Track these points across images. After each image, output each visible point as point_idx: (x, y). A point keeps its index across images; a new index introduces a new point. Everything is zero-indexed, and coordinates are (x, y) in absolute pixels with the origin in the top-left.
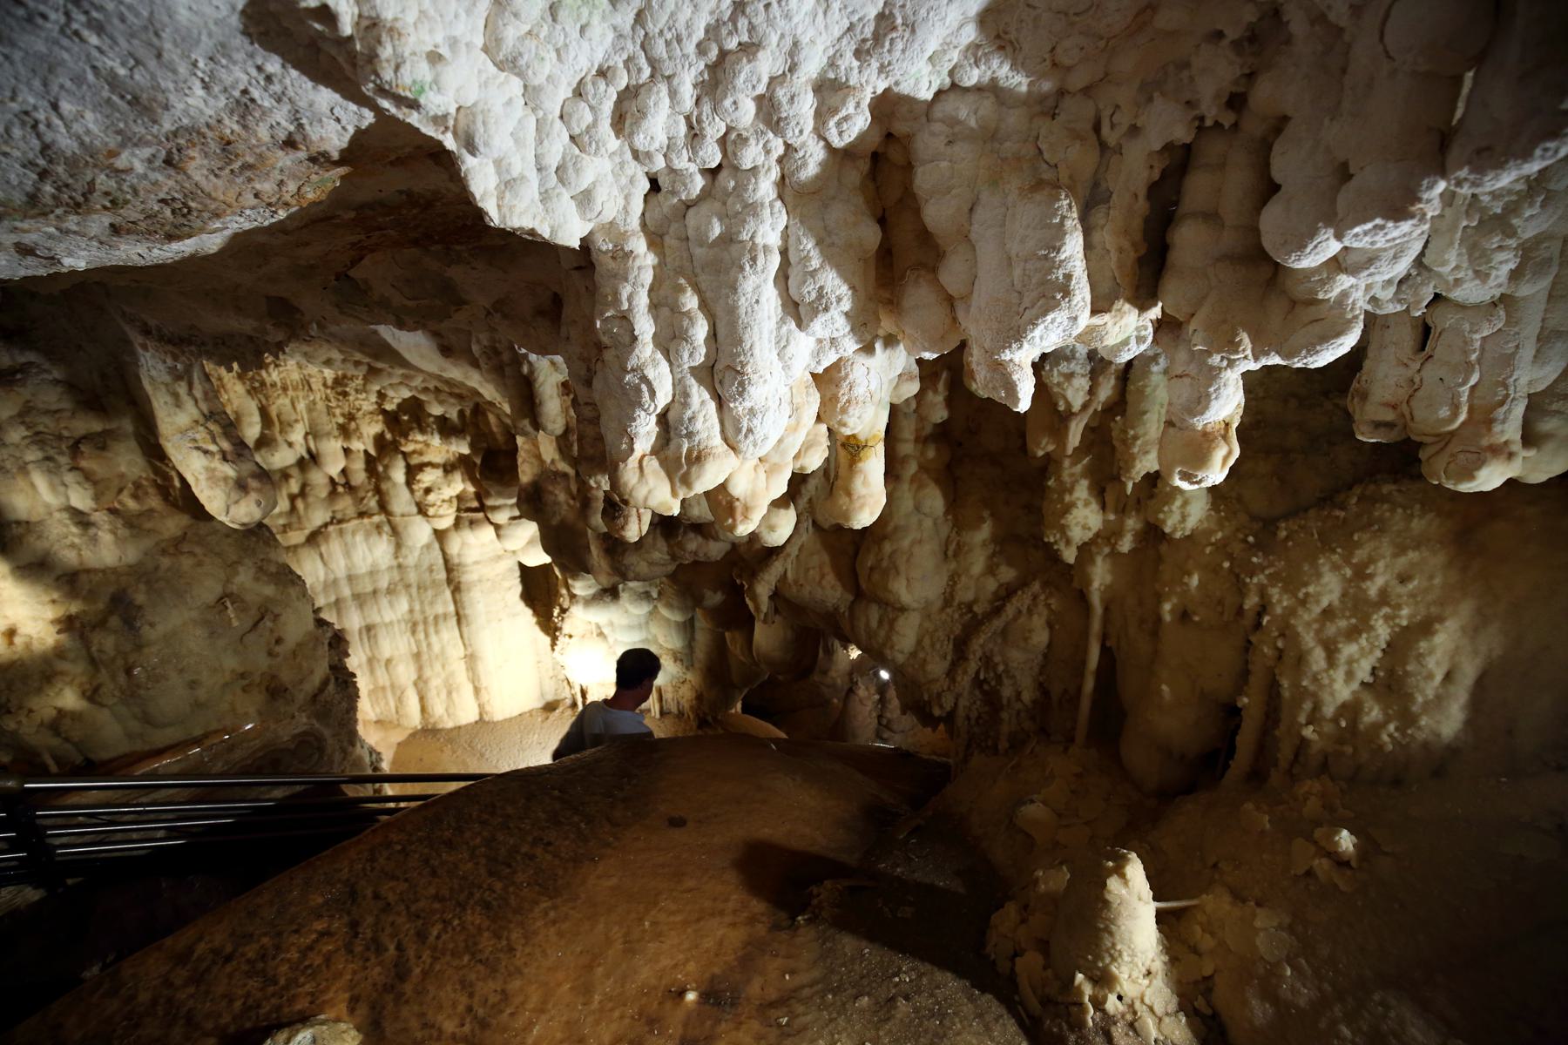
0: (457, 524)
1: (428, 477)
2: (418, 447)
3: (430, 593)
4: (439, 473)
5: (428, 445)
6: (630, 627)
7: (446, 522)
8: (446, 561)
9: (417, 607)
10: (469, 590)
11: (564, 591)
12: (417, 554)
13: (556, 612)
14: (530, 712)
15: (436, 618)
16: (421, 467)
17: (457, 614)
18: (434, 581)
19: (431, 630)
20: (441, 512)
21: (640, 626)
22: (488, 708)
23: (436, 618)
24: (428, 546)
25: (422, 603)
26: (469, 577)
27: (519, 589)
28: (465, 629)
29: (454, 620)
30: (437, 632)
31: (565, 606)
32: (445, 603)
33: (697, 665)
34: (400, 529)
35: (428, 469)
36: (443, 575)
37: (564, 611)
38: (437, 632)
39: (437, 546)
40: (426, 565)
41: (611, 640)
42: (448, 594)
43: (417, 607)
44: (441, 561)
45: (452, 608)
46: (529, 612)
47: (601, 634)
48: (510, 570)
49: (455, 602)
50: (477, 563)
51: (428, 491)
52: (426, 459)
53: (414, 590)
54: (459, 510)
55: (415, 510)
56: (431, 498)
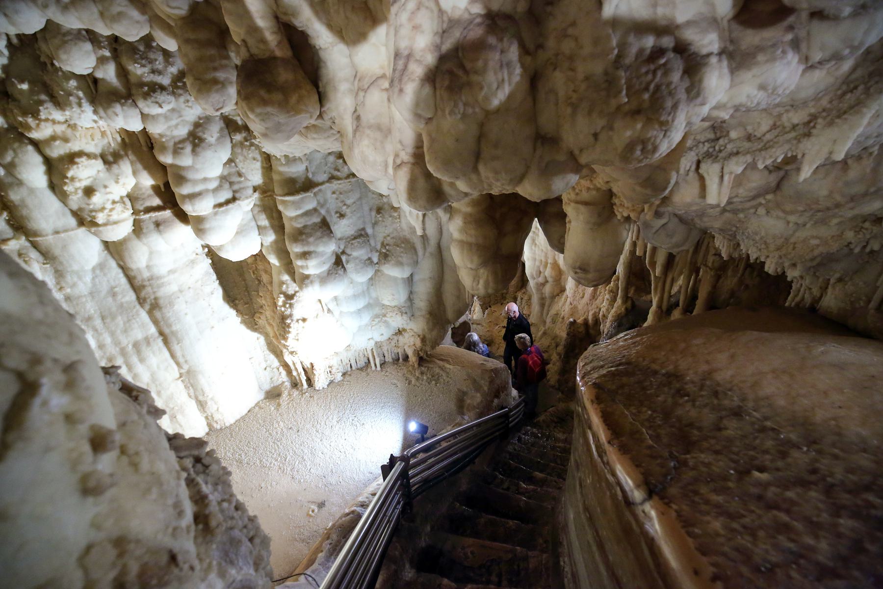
0: (138, 229)
1: (85, 172)
2: (60, 129)
3: (120, 320)
4: (99, 164)
5: (73, 127)
6: (355, 297)
7: (122, 230)
8: (131, 280)
9: (108, 340)
10: (171, 304)
11: (286, 278)
12: (88, 278)
13: (281, 300)
14: (257, 404)
15: (136, 345)
16: (71, 158)
17: (161, 333)
18: (121, 306)
19: (134, 359)
20: (115, 217)
21: (363, 294)
22: (217, 417)
23: (136, 345)
24: (102, 266)
25: (112, 334)
26: (168, 289)
27: (219, 292)
28: (176, 348)
29: (160, 341)
30: (142, 360)
31: (291, 292)
32: (143, 326)
33: (417, 313)
34: (57, 252)
35: (83, 160)
36: (131, 296)
37: (290, 297)
38: (142, 360)
39: (113, 264)
40: (104, 288)
41: (336, 312)
42: (144, 315)
43: (108, 340)
44: (123, 280)
45: (153, 330)
46: (233, 312)
47: (329, 310)
48: (207, 273)
49: (156, 322)
50: (172, 272)
51: (89, 191)
52: (75, 146)
53: (98, 322)
54: (135, 212)
55: (73, 222)
56: (97, 199)
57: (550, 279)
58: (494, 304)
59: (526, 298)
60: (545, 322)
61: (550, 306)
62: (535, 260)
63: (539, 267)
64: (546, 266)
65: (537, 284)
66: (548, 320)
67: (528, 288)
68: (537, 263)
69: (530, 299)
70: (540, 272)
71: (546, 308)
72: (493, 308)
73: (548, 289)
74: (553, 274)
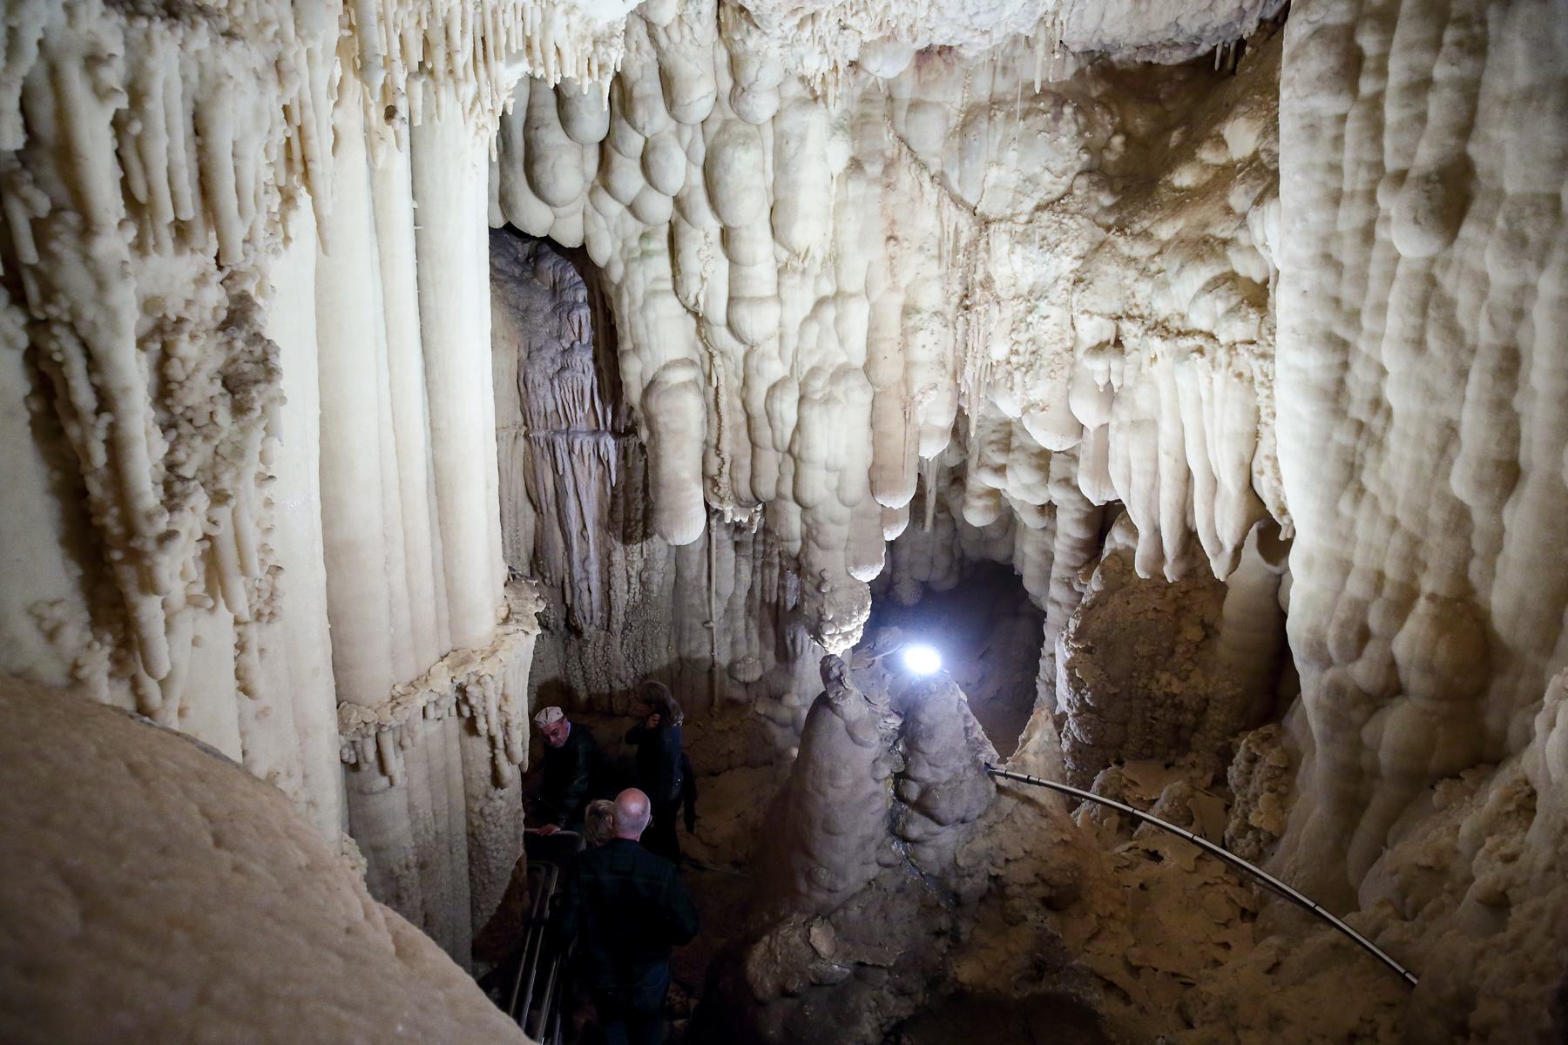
57: (1413, 679)
58: (1139, 756)
59: (1271, 758)
60: (1347, 901)
61: (1389, 820)
62: (1345, 567)
63: (1360, 607)
64: (1402, 606)
65: (1337, 690)
66: (1374, 892)
67: (1292, 723)
68: (1355, 587)
69: (1290, 767)
70: (1364, 635)
71: (1368, 824)
72: (1128, 772)
73: (1393, 730)
74: (1442, 652)
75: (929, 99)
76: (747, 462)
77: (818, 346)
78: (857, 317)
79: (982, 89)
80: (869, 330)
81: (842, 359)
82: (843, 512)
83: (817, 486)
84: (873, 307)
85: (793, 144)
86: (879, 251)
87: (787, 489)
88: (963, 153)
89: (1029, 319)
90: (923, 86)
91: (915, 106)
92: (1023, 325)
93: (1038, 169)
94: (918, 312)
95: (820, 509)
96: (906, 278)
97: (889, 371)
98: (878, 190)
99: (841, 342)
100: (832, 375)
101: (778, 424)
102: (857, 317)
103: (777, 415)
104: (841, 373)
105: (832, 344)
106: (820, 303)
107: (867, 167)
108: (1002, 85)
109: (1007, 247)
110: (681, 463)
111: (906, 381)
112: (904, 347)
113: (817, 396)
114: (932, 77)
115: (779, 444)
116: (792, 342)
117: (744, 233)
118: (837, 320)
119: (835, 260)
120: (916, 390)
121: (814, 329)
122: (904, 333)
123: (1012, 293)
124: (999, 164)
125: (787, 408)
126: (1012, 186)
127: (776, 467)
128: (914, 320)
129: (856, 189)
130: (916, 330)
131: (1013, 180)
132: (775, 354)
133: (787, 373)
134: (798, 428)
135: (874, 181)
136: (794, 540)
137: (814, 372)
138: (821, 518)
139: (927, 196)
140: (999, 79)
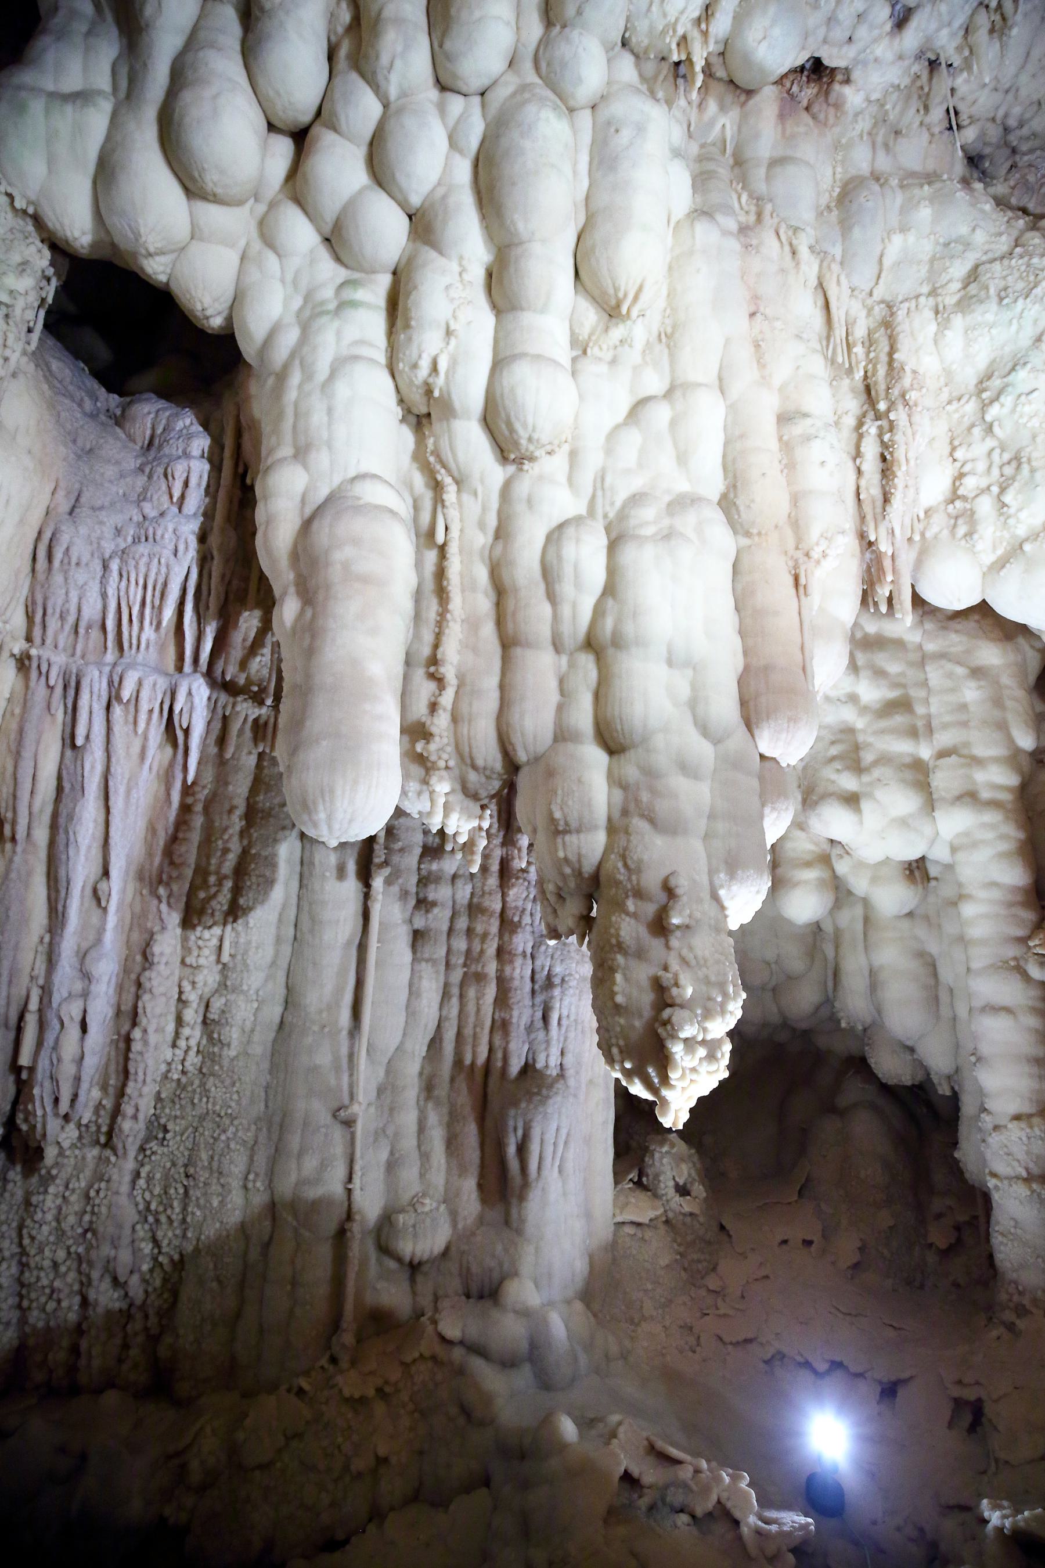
75: (798, 155)
76: (492, 682)
77: (640, 465)
78: (708, 419)
79: (861, 159)
80: (726, 444)
81: (683, 486)
82: (704, 751)
83: (652, 693)
84: (732, 409)
85: (626, 134)
86: (738, 322)
87: (583, 717)
88: (845, 226)
89: (994, 412)
90: (789, 139)
91: (776, 163)
92: (977, 431)
93: (964, 230)
94: (806, 415)
95: (659, 741)
96: (782, 372)
97: (768, 497)
98: (734, 245)
99: (682, 459)
100: (669, 505)
101: (566, 589)
102: (708, 419)
103: (568, 570)
104: (680, 503)
105: (665, 461)
106: (639, 407)
107: (720, 218)
108: (883, 163)
109: (933, 327)
110: (367, 642)
111: (796, 524)
112: (790, 467)
113: (649, 531)
114: (802, 129)
115: (566, 629)
116: (593, 460)
117: (536, 248)
118: (674, 423)
119: (669, 338)
120: (815, 532)
121: (633, 438)
122: (787, 447)
123: (945, 396)
124: (904, 229)
125: (587, 559)
126: (926, 258)
127: (553, 684)
128: (798, 429)
129: (705, 233)
130: (808, 438)
131: (927, 248)
132: (562, 477)
133: (582, 509)
134: (610, 590)
135: (725, 233)
136: (595, 828)
137: (636, 499)
138: (662, 760)
139: (803, 267)
140: (881, 154)
